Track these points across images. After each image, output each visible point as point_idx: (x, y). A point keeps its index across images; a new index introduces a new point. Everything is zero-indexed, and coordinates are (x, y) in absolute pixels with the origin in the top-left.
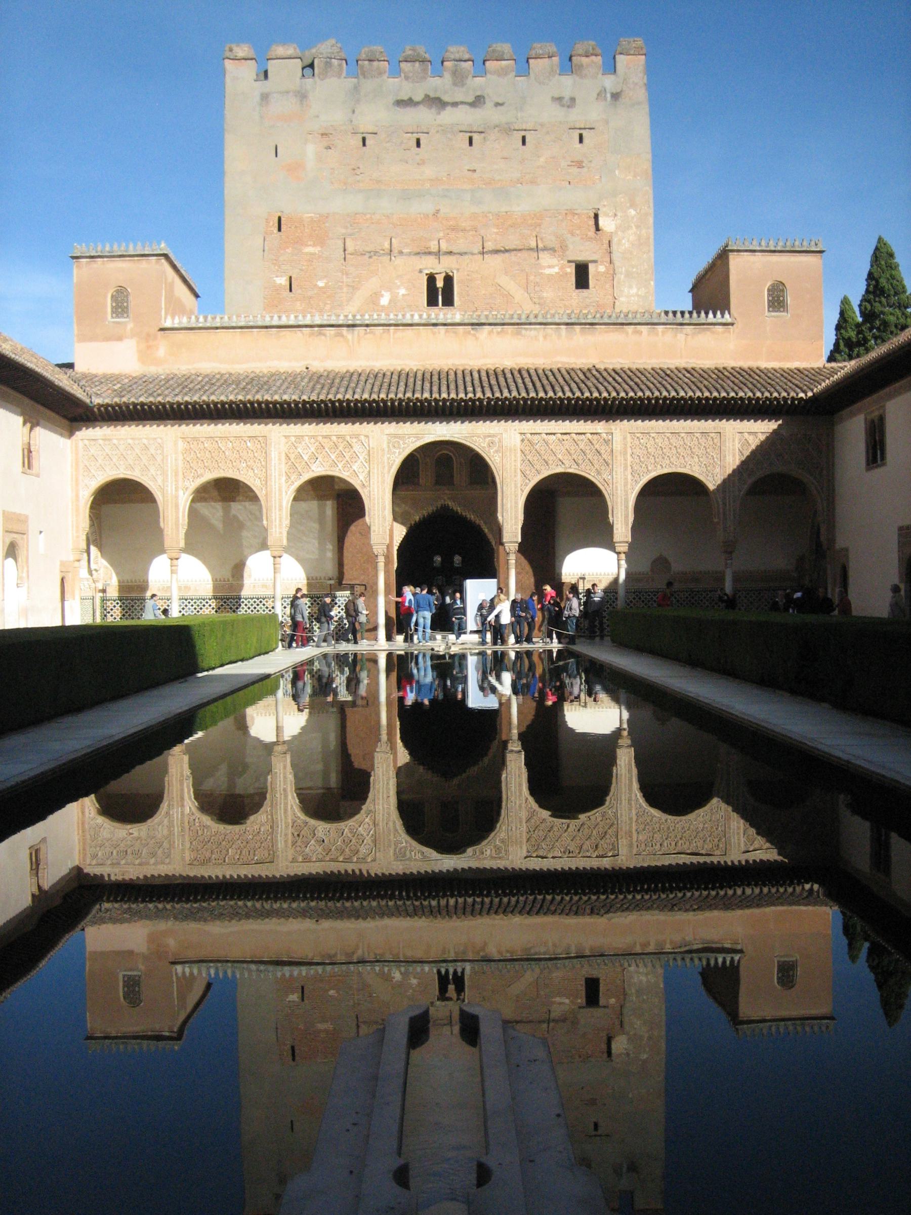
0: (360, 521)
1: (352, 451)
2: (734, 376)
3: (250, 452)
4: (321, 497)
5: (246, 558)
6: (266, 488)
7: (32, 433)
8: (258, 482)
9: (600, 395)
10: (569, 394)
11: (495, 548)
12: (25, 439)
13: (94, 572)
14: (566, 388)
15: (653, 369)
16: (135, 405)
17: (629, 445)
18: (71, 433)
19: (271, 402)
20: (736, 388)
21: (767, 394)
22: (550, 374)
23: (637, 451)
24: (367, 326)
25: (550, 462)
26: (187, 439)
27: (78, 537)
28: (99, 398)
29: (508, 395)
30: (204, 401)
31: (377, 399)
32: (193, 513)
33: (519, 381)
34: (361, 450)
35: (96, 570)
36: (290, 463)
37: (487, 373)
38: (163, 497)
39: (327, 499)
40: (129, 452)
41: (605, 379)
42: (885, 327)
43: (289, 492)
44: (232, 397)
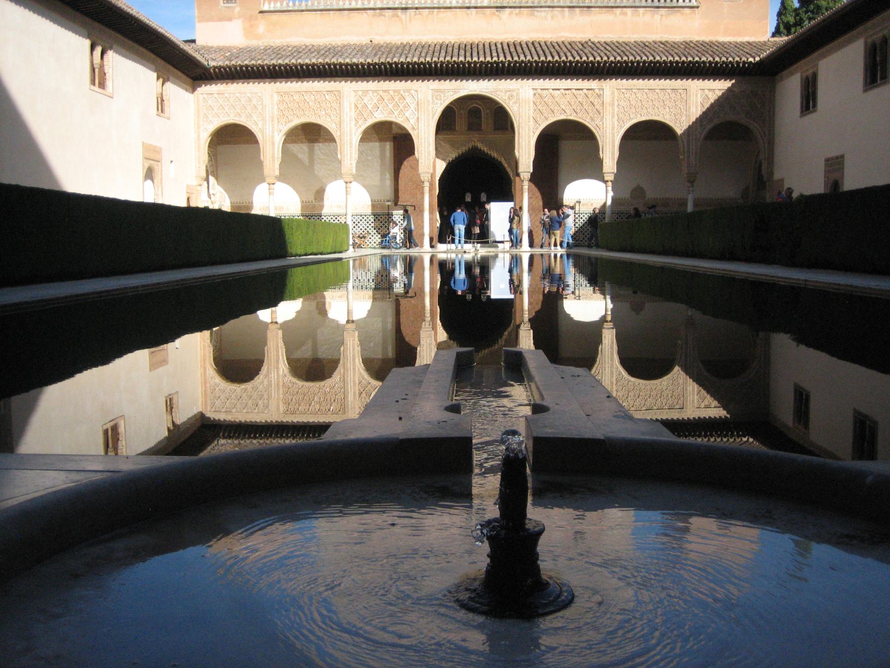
0: (411, 158)
1: (405, 103)
2: (698, 47)
3: (328, 102)
4: (381, 140)
5: (326, 186)
6: (340, 130)
7: (164, 86)
8: (334, 126)
9: (595, 59)
10: (570, 58)
11: (512, 178)
12: (158, 90)
13: (212, 196)
14: (569, 54)
15: (635, 42)
16: (241, 67)
17: (616, 98)
18: (194, 90)
19: (344, 64)
20: (700, 55)
21: (724, 59)
22: (556, 45)
23: (622, 103)
24: (417, 8)
25: (556, 111)
26: (281, 94)
27: (199, 167)
28: (212, 62)
29: (524, 59)
30: (293, 63)
31: (424, 62)
32: (284, 151)
33: (533, 50)
34: (412, 101)
35: (214, 195)
36: (358, 111)
37: (508, 45)
38: (263, 137)
39: (388, 141)
40: (237, 103)
41: (598, 48)
42: (818, 9)
43: (357, 134)
44: (314, 61)
